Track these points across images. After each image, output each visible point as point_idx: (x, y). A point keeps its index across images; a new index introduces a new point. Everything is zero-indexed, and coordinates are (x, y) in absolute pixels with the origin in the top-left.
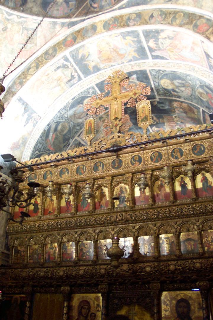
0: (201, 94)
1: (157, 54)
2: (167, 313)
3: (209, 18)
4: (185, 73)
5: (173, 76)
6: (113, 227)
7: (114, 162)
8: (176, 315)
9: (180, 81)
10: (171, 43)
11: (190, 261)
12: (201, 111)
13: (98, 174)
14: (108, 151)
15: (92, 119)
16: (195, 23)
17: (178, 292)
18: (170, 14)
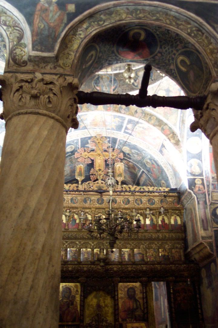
0: (147, 162)
1: (128, 132)
2: (122, 295)
3: (171, 127)
4: (143, 148)
5: (134, 147)
6: (93, 241)
7: (98, 200)
8: (127, 297)
9: (137, 151)
10: (142, 131)
11: (140, 266)
12: (142, 170)
13: (87, 205)
14: (96, 191)
15: (81, 165)
16: (163, 127)
17: (128, 284)
18: (148, 114)
